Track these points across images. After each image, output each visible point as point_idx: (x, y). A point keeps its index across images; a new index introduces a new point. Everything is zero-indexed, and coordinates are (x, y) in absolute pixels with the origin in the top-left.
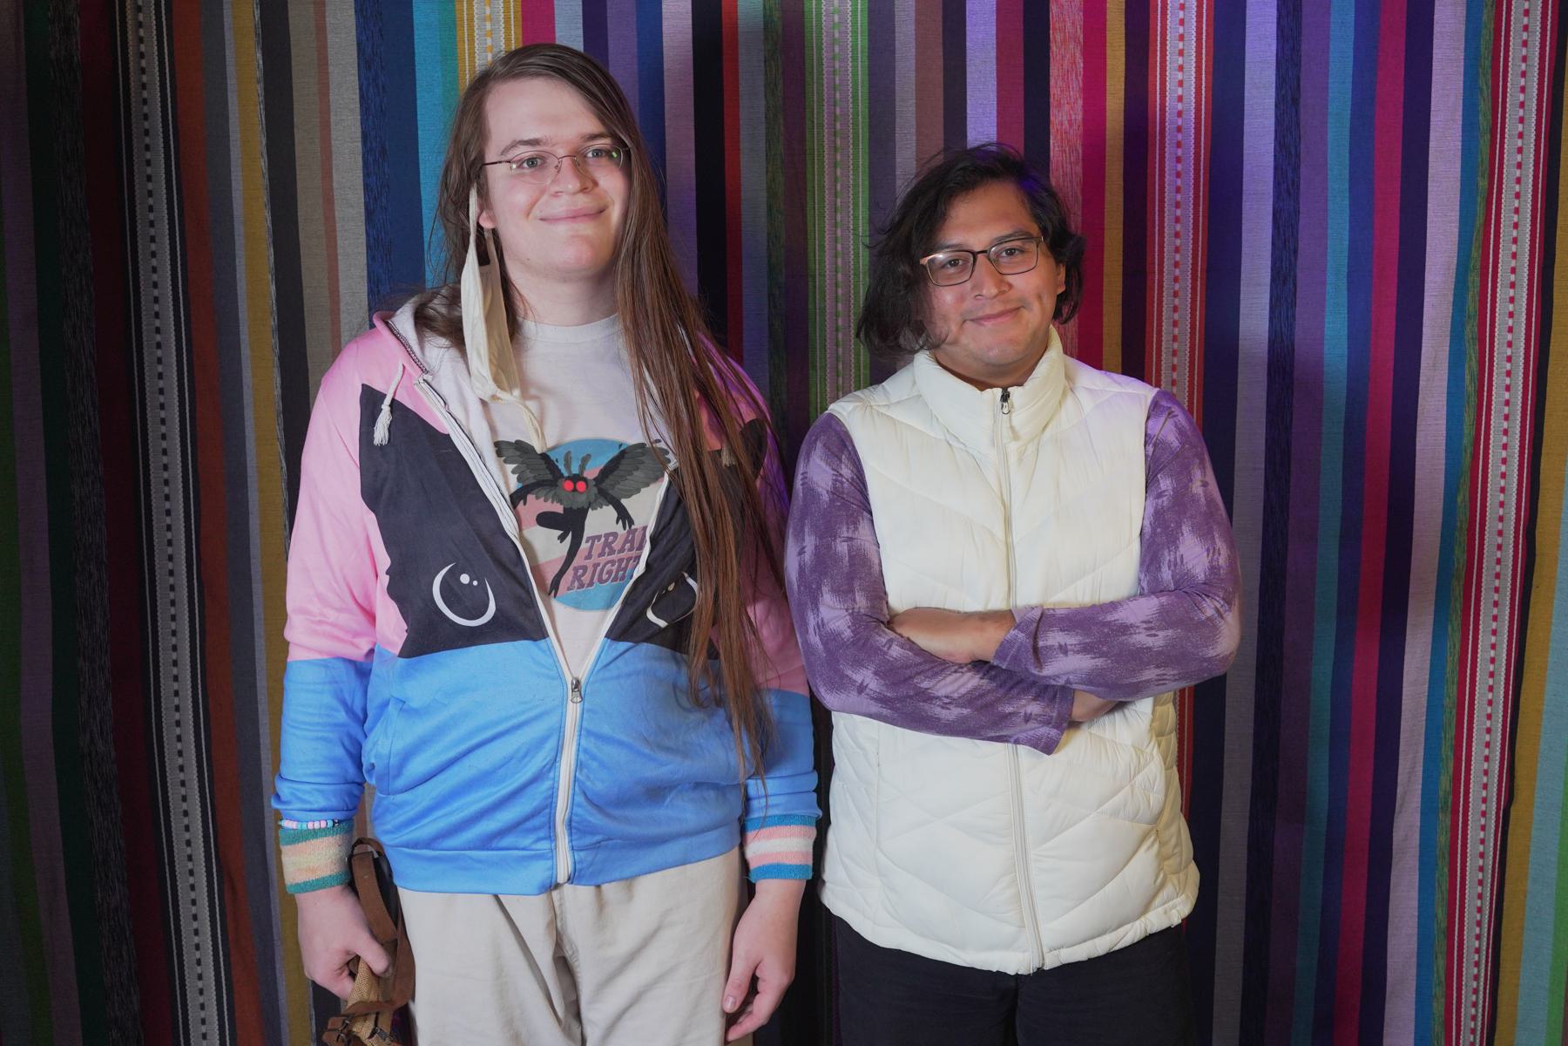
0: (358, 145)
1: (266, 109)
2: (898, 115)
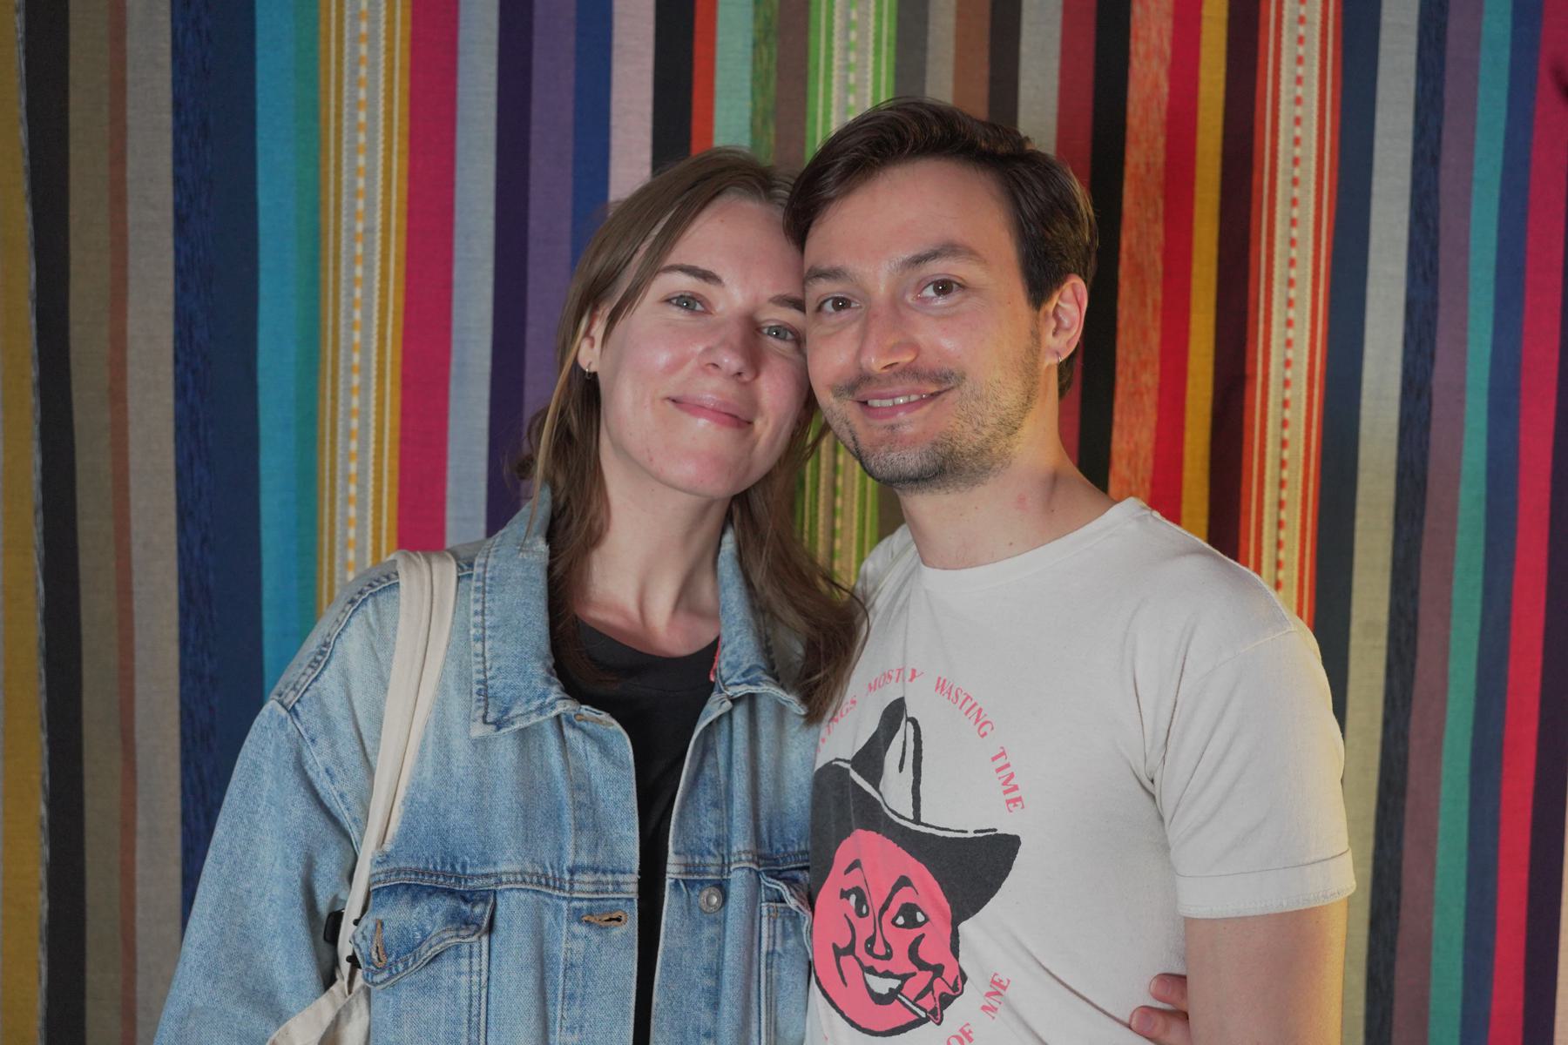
0: (167, 118)
1: (27, 52)
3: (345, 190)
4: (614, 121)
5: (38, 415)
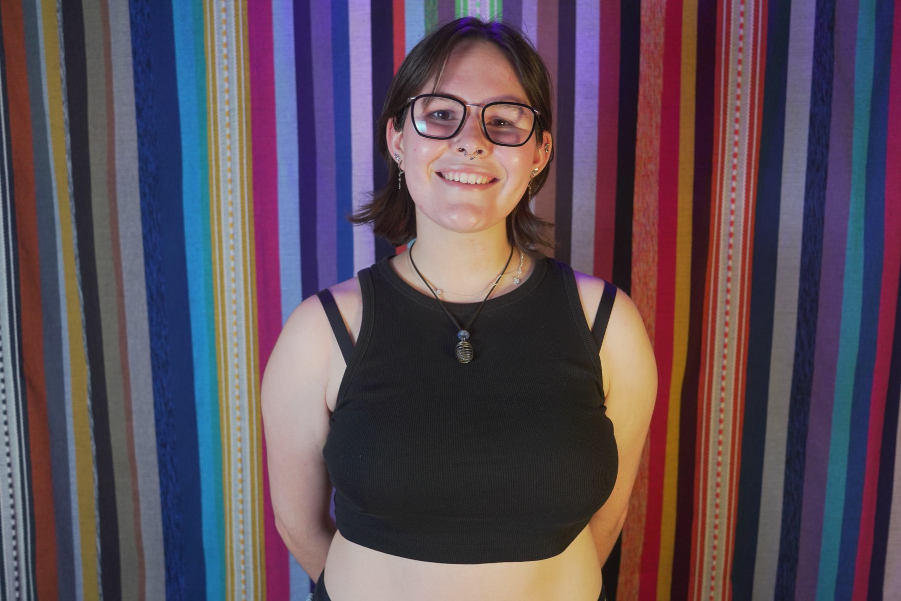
1: (64, 32)
3: (218, 90)
4: (352, 43)
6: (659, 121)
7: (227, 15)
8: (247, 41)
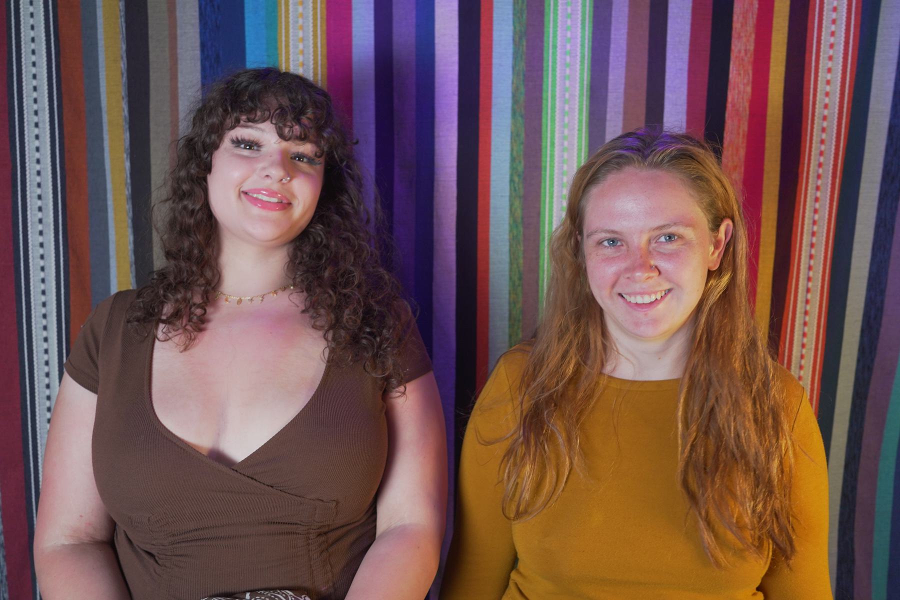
0: (198, 53)
1: (126, 22)
2: (612, 41)
5: (131, 214)
6: (746, 129)
7: (304, 8)
8: (325, 36)
